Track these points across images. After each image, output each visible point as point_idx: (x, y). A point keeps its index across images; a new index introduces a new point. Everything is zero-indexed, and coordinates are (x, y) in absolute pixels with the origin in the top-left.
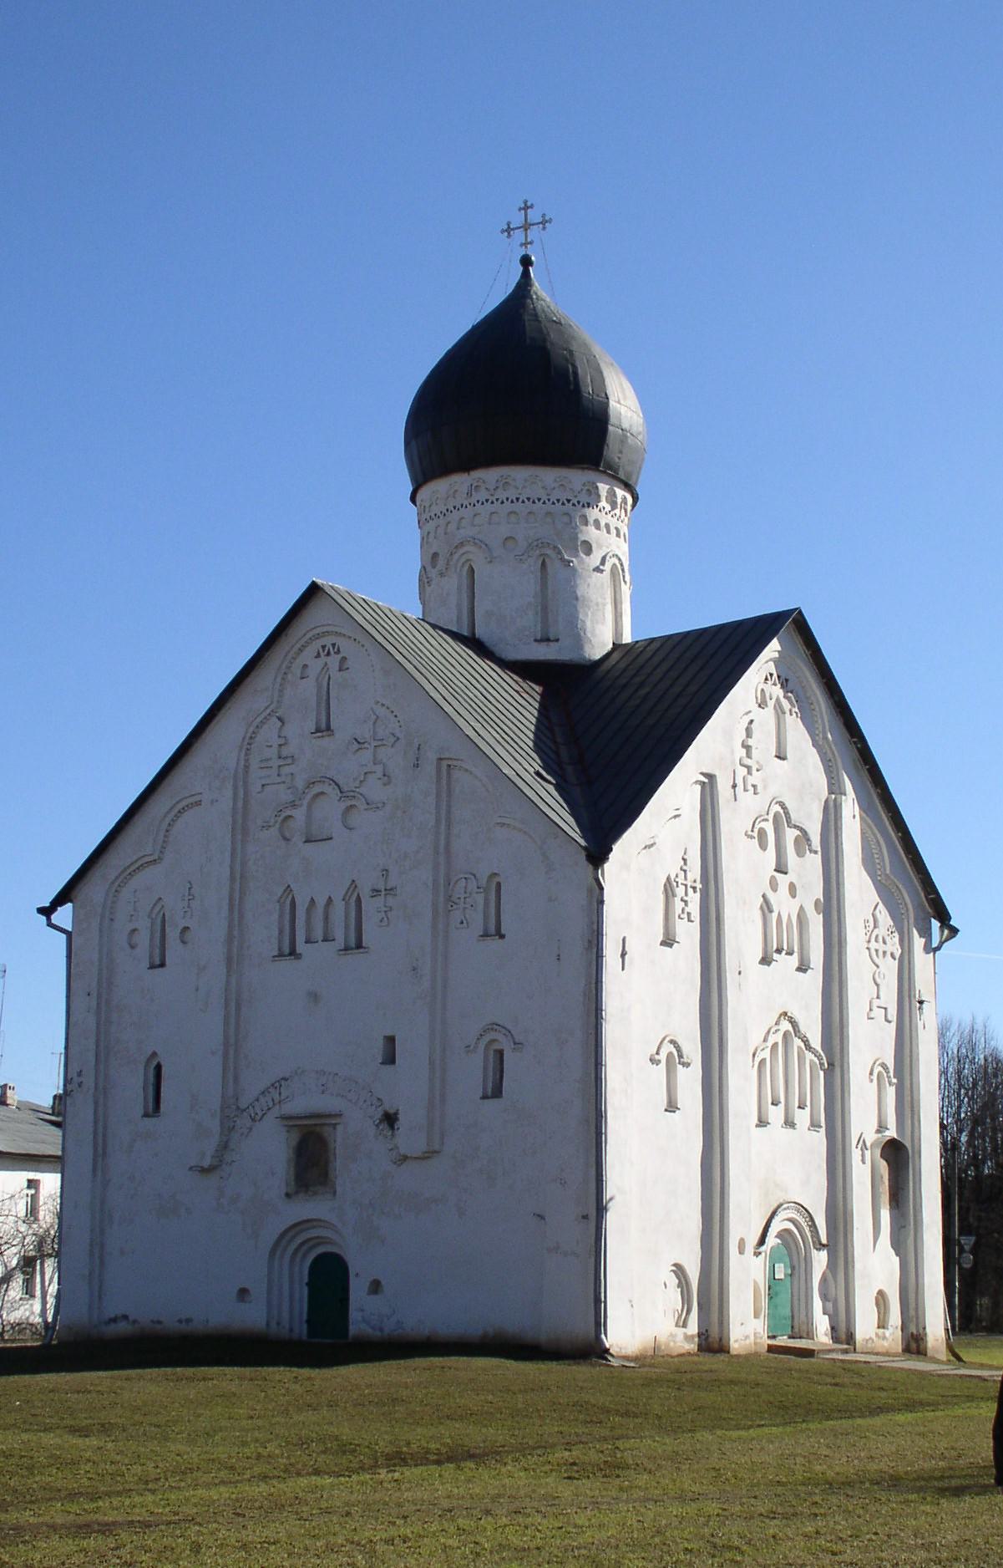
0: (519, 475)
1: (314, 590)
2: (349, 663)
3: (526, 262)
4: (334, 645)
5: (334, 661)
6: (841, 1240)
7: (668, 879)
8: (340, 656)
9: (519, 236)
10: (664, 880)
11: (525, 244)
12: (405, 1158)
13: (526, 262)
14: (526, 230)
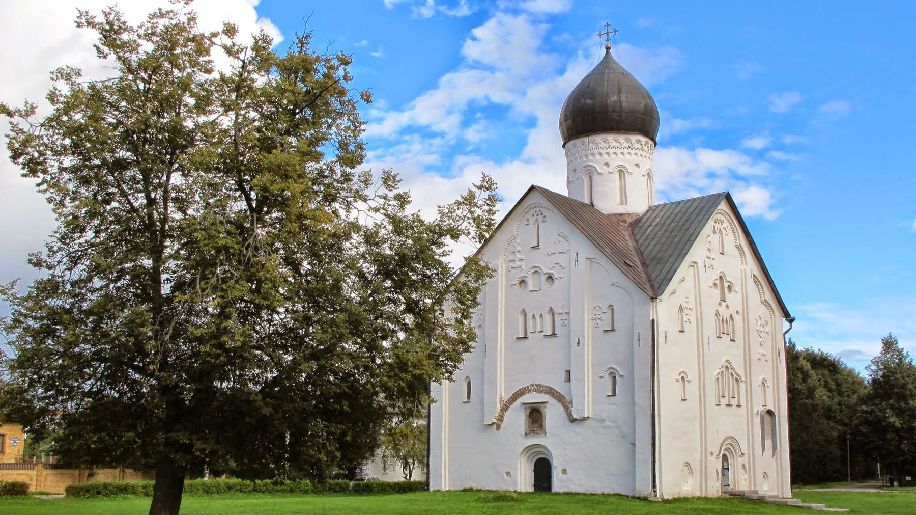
0: (611, 138)
1: (533, 188)
2: (547, 219)
3: (608, 48)
5: (540, 218)
7: (681, 305)
10: (679, 306)
11: (608, 40)
12: (575, 420)
14: (608, 34)
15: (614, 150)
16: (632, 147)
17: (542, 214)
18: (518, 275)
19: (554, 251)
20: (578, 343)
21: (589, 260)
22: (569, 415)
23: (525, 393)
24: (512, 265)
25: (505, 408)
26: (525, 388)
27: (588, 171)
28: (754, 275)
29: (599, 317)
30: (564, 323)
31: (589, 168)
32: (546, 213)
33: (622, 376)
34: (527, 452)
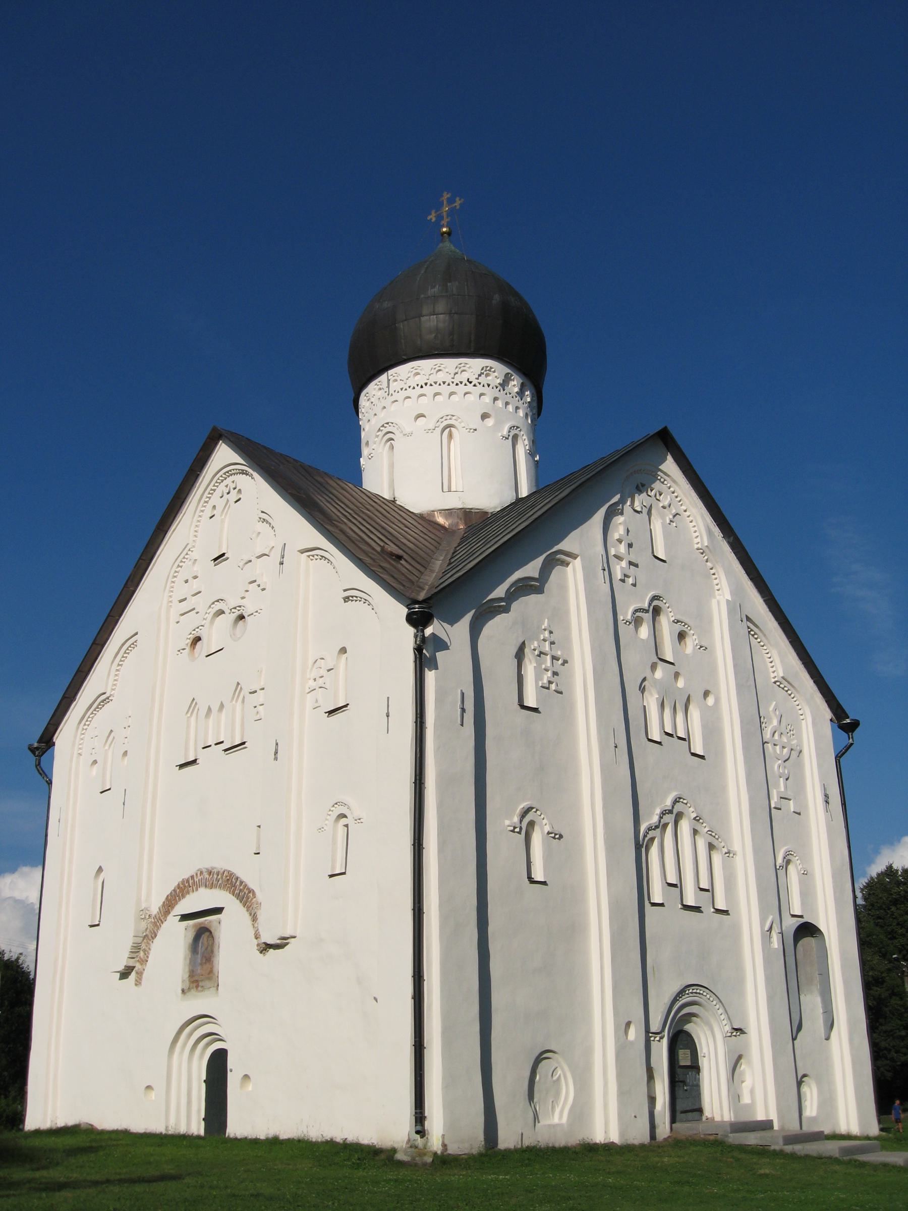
8: (236, 490)
15: (436, 389)
16: (475, 382)
17: (234, 489)
18: (189, 625)
19: (246, 559)
20: (276, 753)
22: (257, 937)
23: (188, 893)
25: (150, 936)
26: (188, 881)
28: (748, 619)
29: (320, 682)
31: (389, 429)
32: (242, 481)
33: (358, 820)
34: (191, 1034)
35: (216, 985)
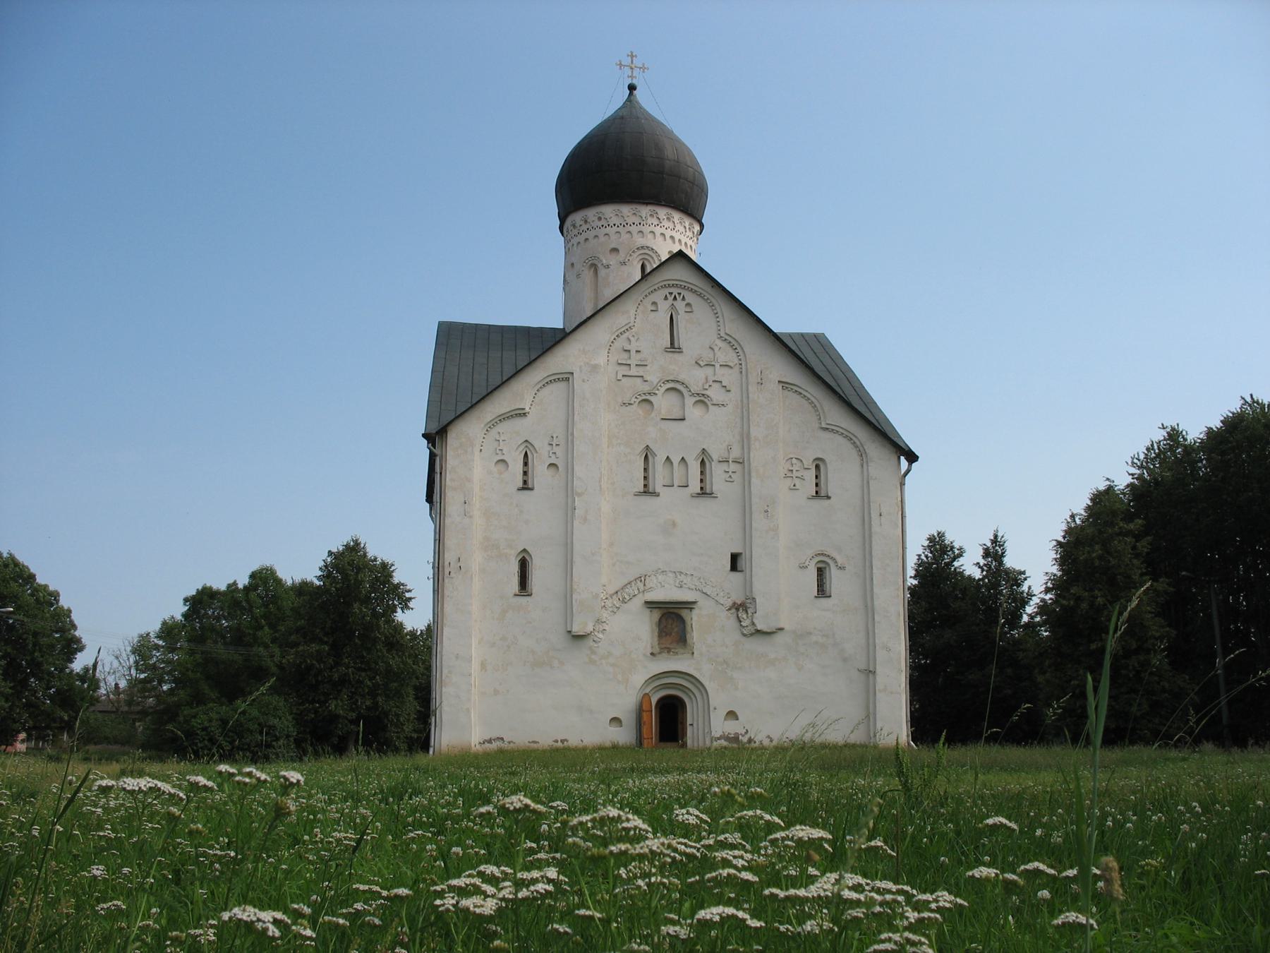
3: (632, 88)
4: (679, 294)
5: (680, 305)
6: (434, 657)
9: (628, 71)
13: (632, 88)
21: (781, 385)
24: (624, 370)
27: (647, 257)
29: (799, 474)
30: (730, 476)
32: (690, 298)
35: (691, 652)
